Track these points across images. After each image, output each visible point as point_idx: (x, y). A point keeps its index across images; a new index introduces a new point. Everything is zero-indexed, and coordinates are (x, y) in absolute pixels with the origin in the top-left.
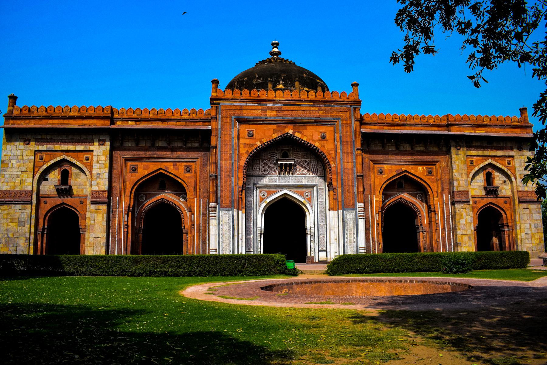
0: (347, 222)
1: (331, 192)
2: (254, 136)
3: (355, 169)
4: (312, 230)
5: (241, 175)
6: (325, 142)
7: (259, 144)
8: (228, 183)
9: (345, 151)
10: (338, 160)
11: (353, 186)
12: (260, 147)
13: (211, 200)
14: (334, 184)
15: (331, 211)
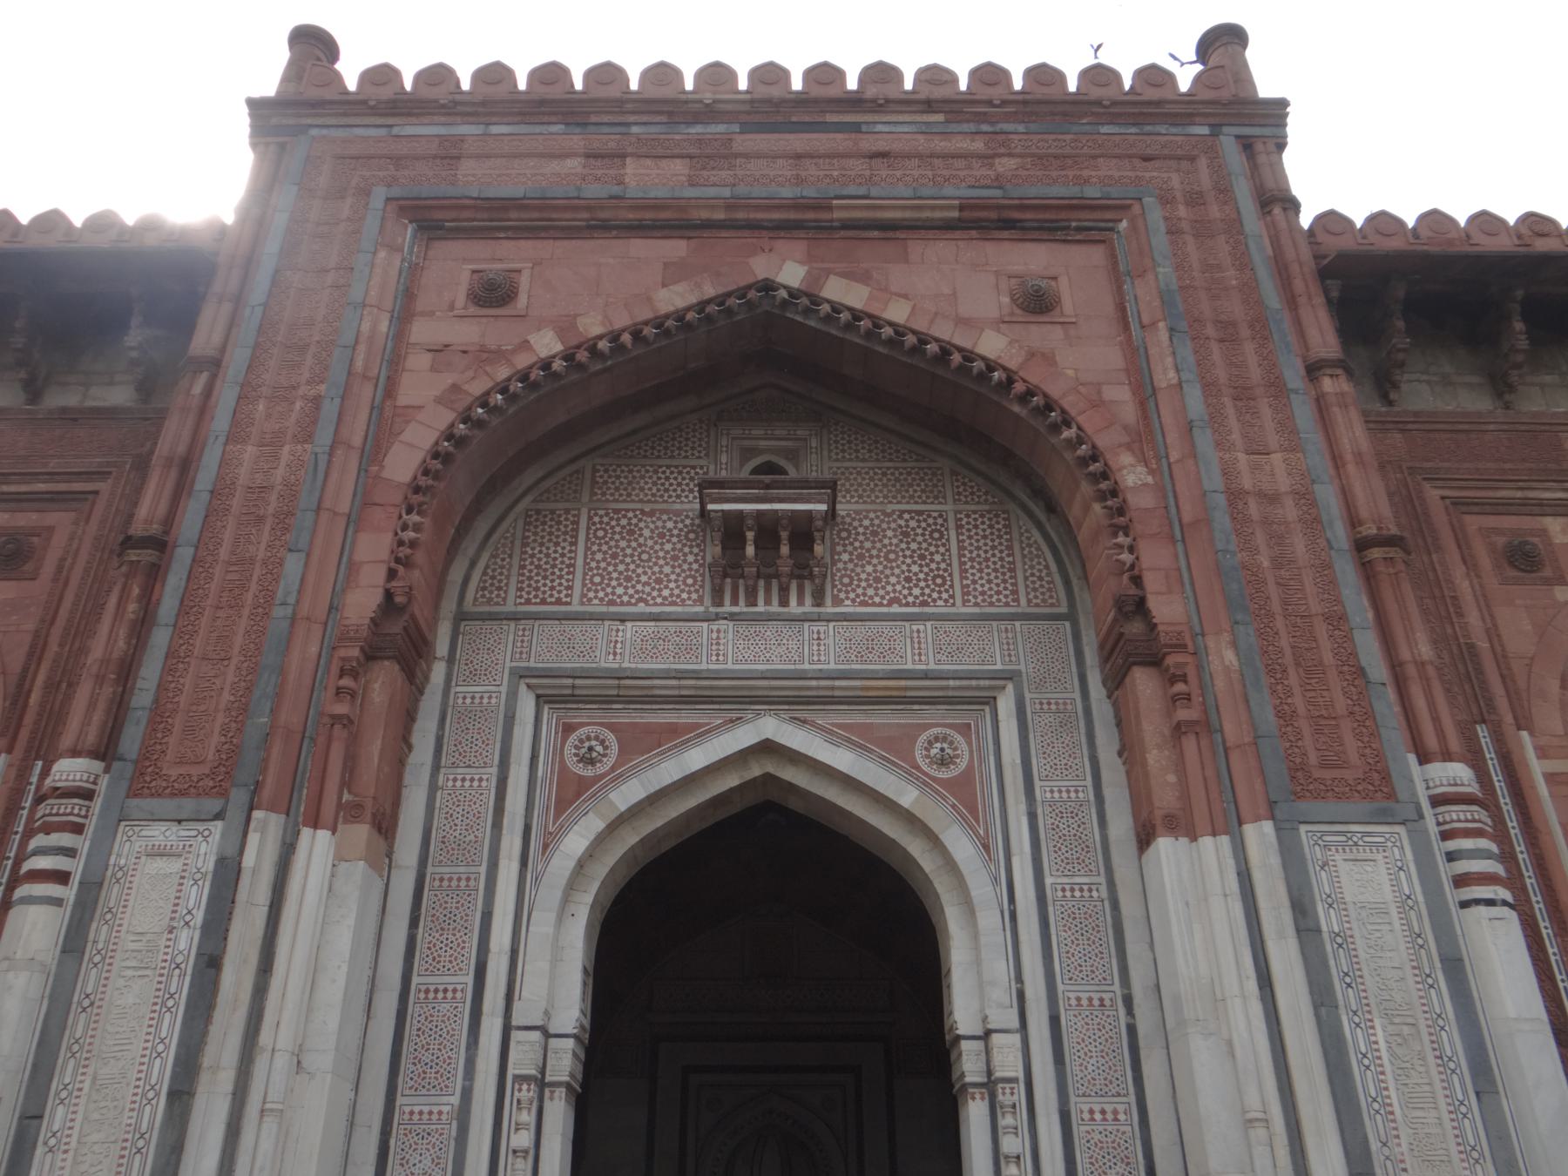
0: (1343, 940)
1: (1143, 682)
2: (522, 300)
3: (1327, 495)
4: (1008, 1062)
5: (374, 548)
6: (1058, 330)
7: (547, 344)
8: (249, 596)
9: (1221, 374)
10: (1172, 437)
11: (1337, 620)
12: (558, 365)
13: (67, 740)
14: (1166, 609)
15: (1164, 845)
